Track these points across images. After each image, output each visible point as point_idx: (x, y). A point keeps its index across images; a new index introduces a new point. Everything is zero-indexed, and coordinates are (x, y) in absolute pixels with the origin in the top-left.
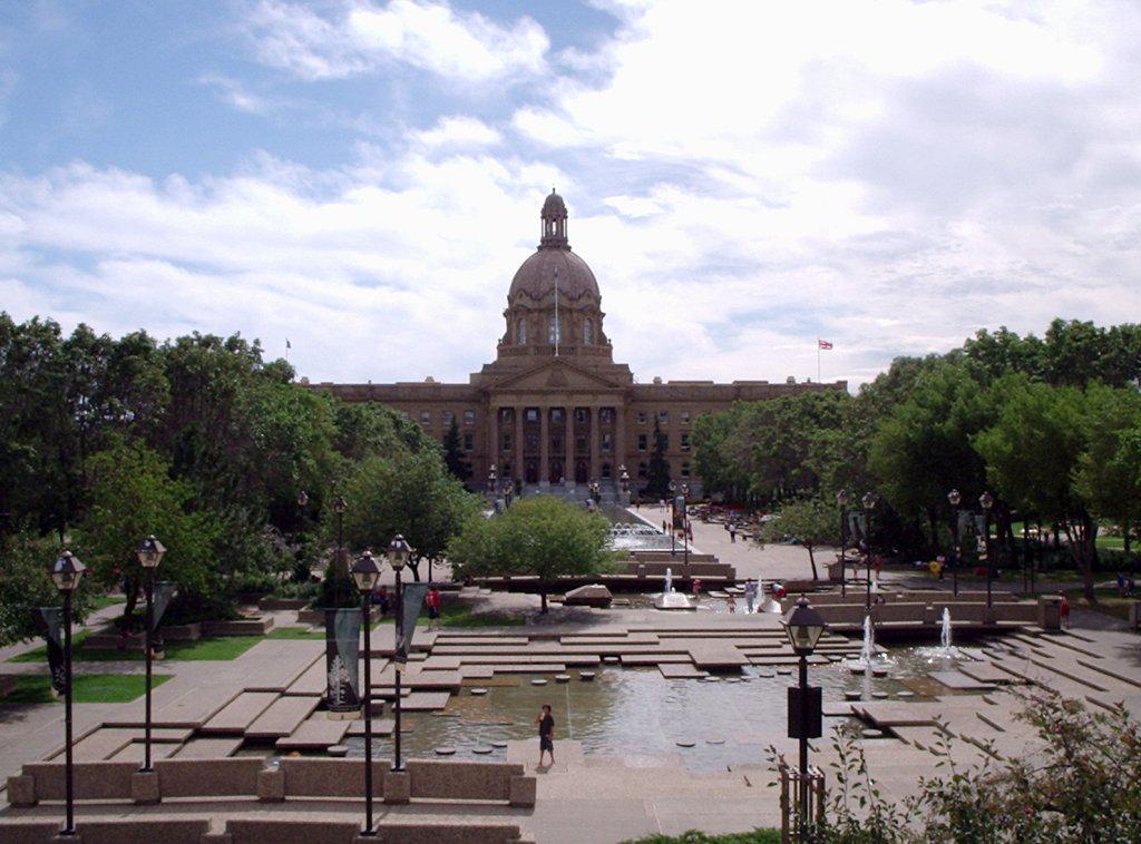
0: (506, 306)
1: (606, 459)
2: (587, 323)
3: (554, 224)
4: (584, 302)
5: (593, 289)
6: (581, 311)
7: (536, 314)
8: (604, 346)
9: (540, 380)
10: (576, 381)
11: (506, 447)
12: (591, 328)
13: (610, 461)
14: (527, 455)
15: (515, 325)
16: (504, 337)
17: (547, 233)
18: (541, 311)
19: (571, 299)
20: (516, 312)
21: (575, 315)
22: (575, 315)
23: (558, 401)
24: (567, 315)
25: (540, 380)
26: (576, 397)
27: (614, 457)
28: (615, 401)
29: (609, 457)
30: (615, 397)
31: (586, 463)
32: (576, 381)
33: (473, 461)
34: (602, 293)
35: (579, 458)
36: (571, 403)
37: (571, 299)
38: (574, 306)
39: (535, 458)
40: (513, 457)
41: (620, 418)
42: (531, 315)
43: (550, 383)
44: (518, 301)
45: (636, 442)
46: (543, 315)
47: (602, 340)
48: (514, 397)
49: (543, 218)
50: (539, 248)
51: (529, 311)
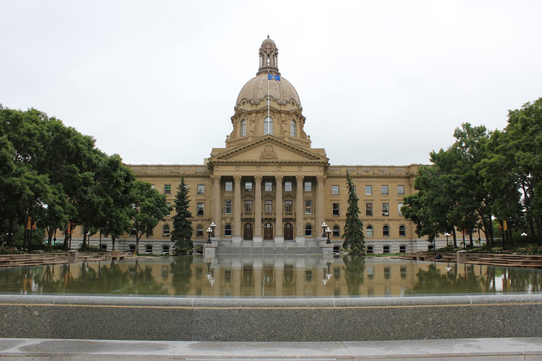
0: (233, 113)
1: (309, 221)
2: (292, 123)
3: (268, 60)
4: (290, 108)
5: (296, 99)
6: (288, 113)
7: (254, 115)
8: (305, 139)
9: (254, 155)
10: (284, 155)
11: (228, 210)
12: (295, 126)
13: (312, 222)
14: (244, 216)
15: (239, 125)
16: (231, 134)
17: (263, 64)
18: (257, 112)
19: (280, 105)
20: (240, 115)
21: (283, 115)
22: (283, 115)
23: (269, 172)
24: (278, 115)
25: (254, 155)
26: (284, 168)
27: (314, 219)
28: (316, 172)
29: (312, 219)
30: (316, 168)
31: (293, 224)
32: (284, 155)
33: (204, 223)
34: (303, 105)
35: (286, 219)
36: (279, 173)
37: (280, 105)
38: (283, 109)
39: (251, 219)
40: (232, 219)
41: (320, 185)
42: (250, 116)
43: (262, 157)
44: (242, 107)
45: (331, 209)
46: (259, 115)
47: (303, 134)
48: (233, 168)
49: (261, 54)
50: (258, 74)
51: (250, 113)
